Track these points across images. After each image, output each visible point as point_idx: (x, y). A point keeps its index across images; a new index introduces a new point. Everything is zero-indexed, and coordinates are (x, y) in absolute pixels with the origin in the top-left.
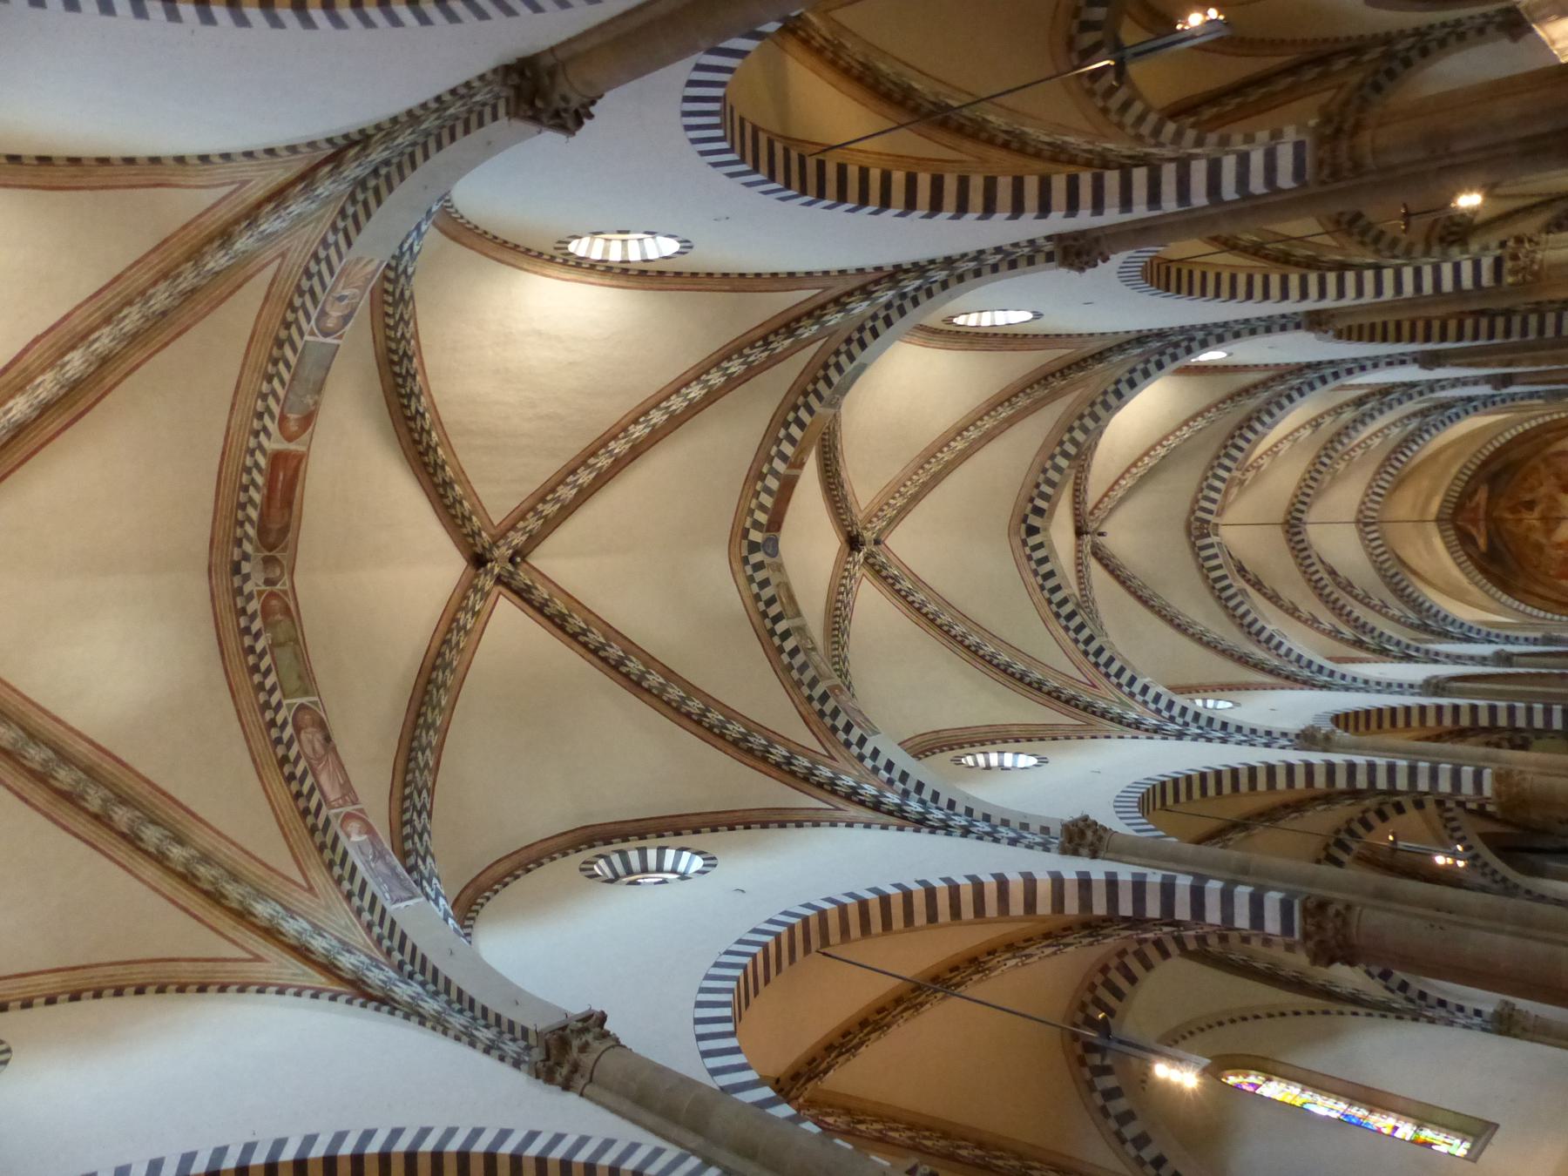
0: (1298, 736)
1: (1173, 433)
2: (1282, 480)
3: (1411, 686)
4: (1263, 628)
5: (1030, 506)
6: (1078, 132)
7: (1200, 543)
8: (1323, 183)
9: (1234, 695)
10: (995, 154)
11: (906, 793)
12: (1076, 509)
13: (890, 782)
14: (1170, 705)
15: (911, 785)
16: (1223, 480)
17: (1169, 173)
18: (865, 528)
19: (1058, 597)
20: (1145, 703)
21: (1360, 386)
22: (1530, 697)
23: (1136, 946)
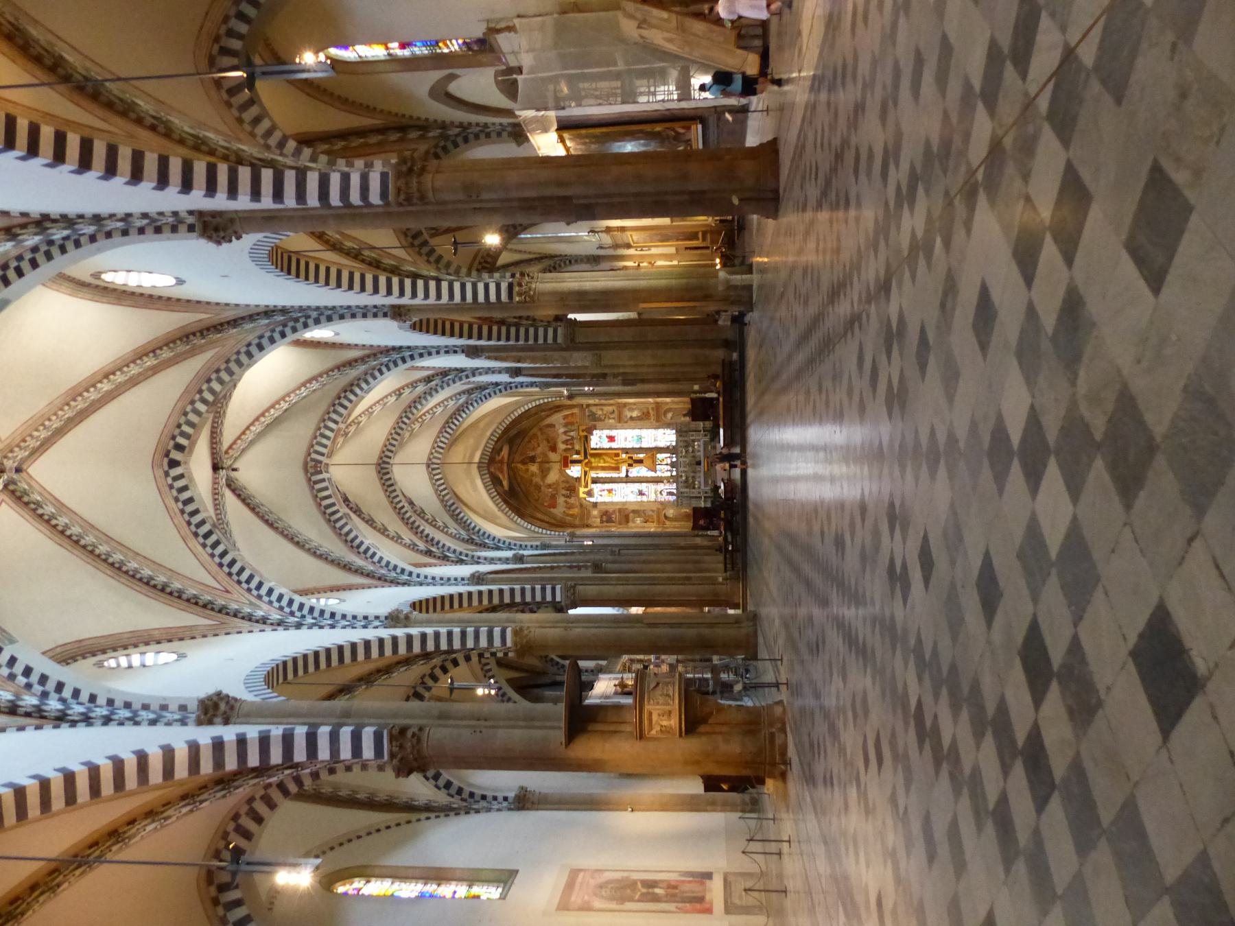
0: (386, 618)
1: (294, 391)
2: (376, 434)
3: (463, 579)
4: (362, 543)
5: (172, 443)
6: (217, 131)
7: (314, 478)
8: (401, 205)
9: (342, 594)
10: (144, 134)
11: (45, 695)
12: (212, 448)
13: (29, 686)
14: (291, 602)
15: (51, 686)
16: (332, 430)
17: (290, 178)
18: (6, 457)
19: (196, 519)
20: (270, 603)
21: (428, 368)
22: (533, 581)
23: (262, 792)
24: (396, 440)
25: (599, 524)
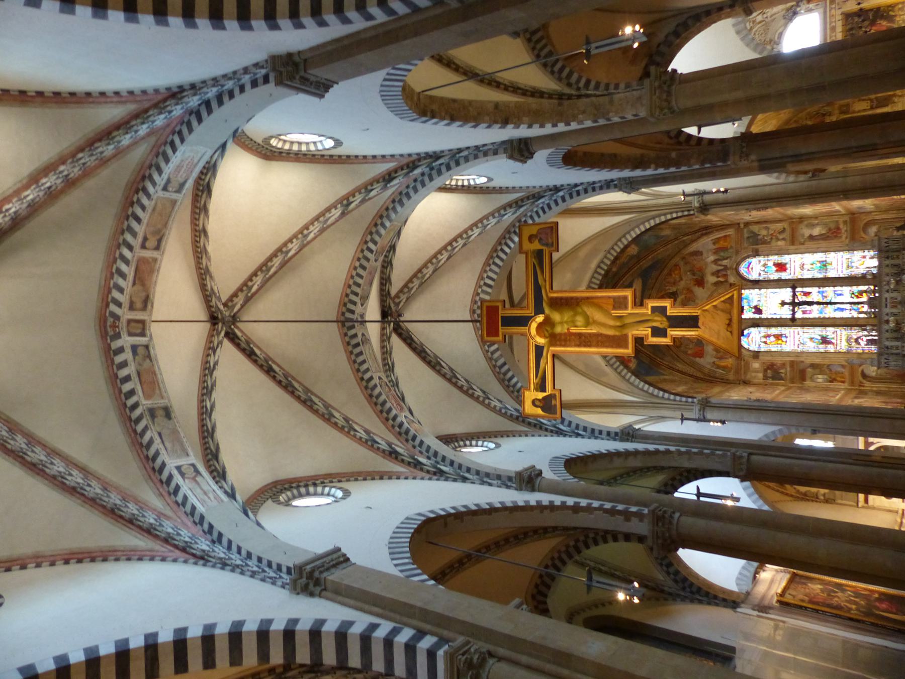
24: (361, 277)
25: (761, 381)
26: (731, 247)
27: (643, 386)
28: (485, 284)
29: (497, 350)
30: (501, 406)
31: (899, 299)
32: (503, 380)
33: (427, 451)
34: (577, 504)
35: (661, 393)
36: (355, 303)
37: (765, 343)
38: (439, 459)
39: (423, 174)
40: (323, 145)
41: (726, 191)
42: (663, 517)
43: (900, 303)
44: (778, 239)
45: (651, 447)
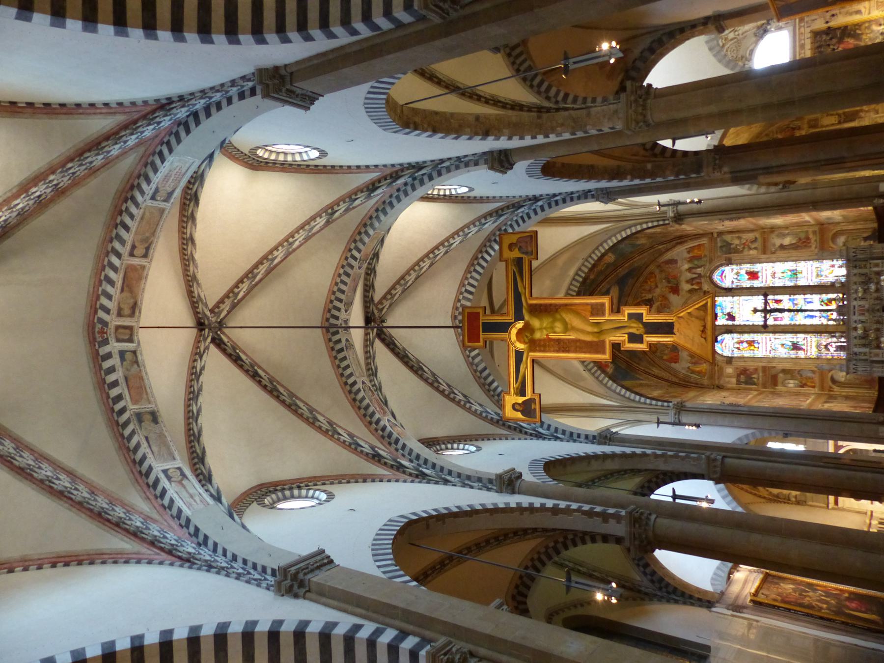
24: (345, 284)
25: (735, 386)
26: (705, 256)
27: (620, 391)
28: (467, 291)
29: (478, 355)
30: (482, 410)
31: (867, 306)
32: (484, 385)
33: (410, 454)
34: (556, 506)
35: (638, 398)
36: (339, 310)
37: (738, 348)
38: (421, 462)
39: (406, 184)
40: (308, 155)
41: (700, 202)
42: (640, 518)
43: (868, 310)
44: (750, 249)
45: (628, 450)
